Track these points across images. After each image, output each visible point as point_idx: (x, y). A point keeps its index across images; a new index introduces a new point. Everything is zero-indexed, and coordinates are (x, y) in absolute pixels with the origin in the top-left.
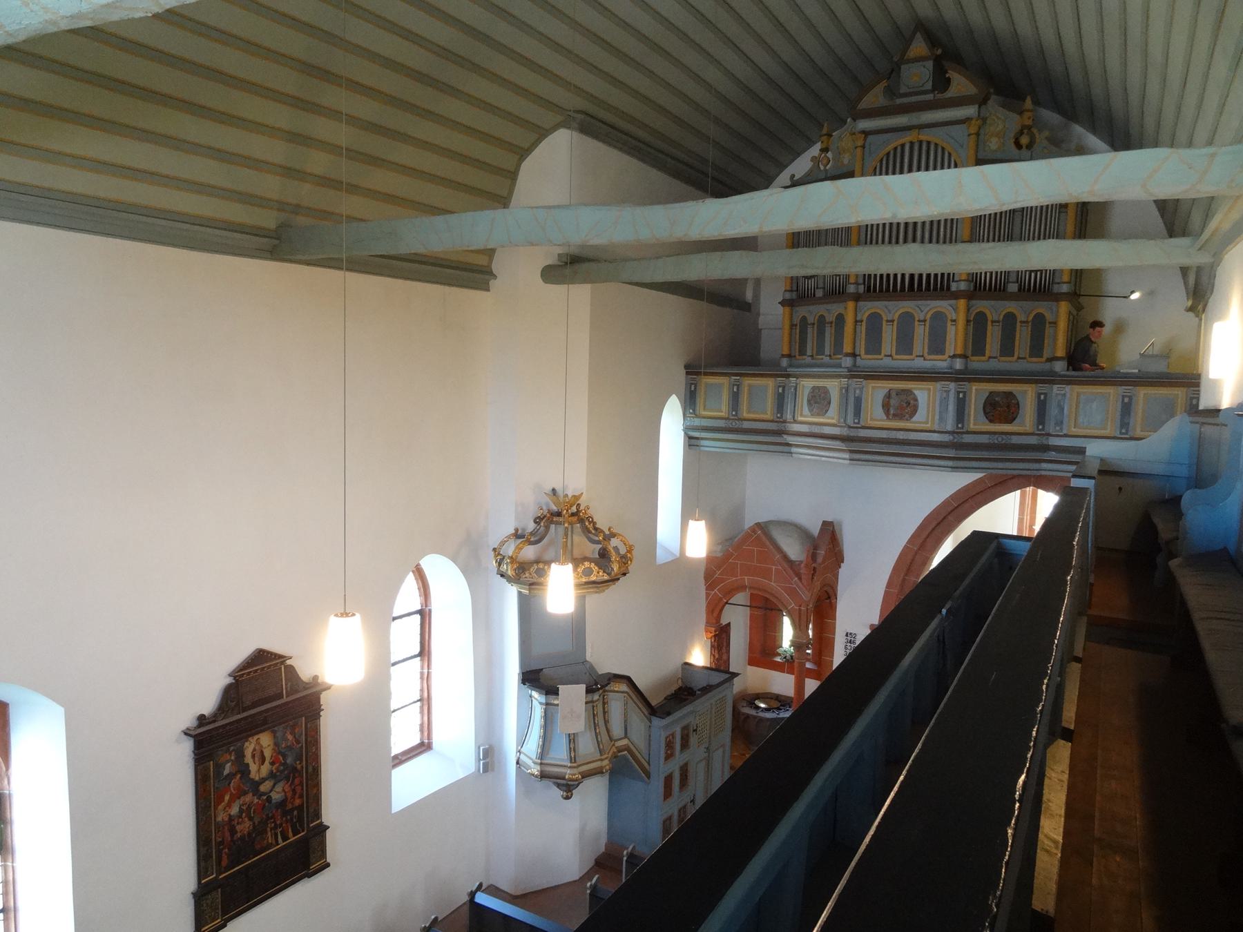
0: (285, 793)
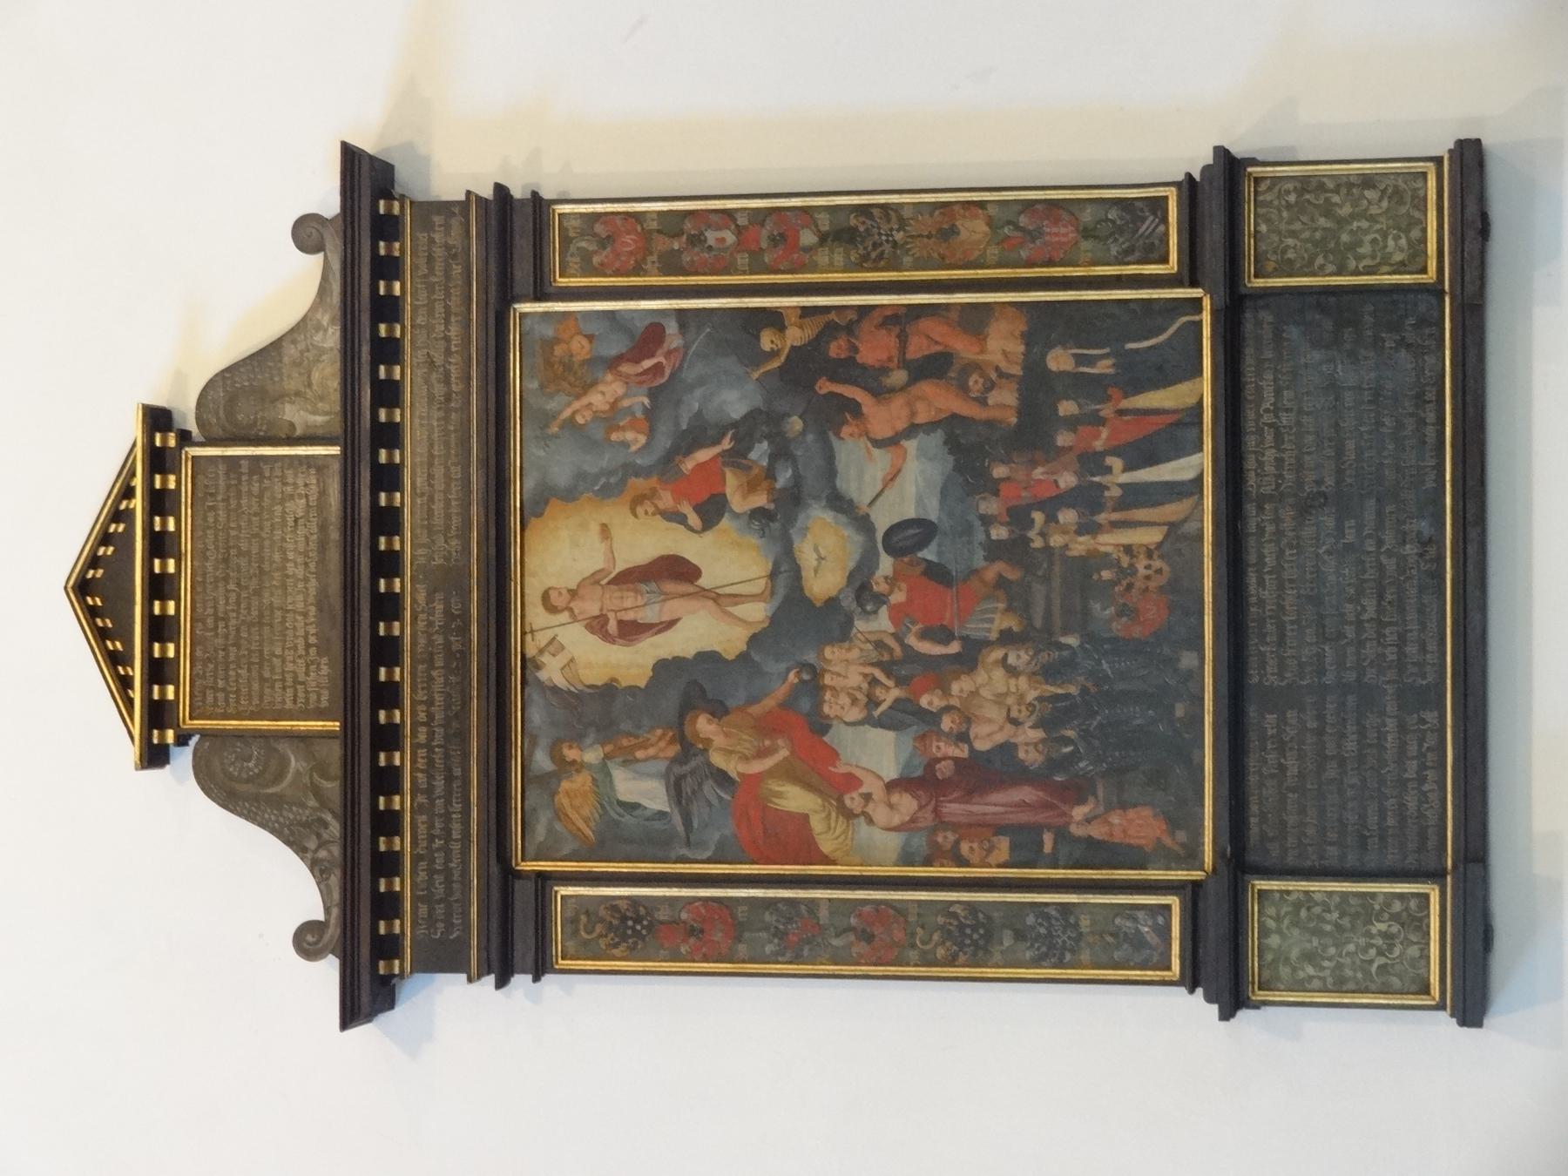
0: (912, 430)
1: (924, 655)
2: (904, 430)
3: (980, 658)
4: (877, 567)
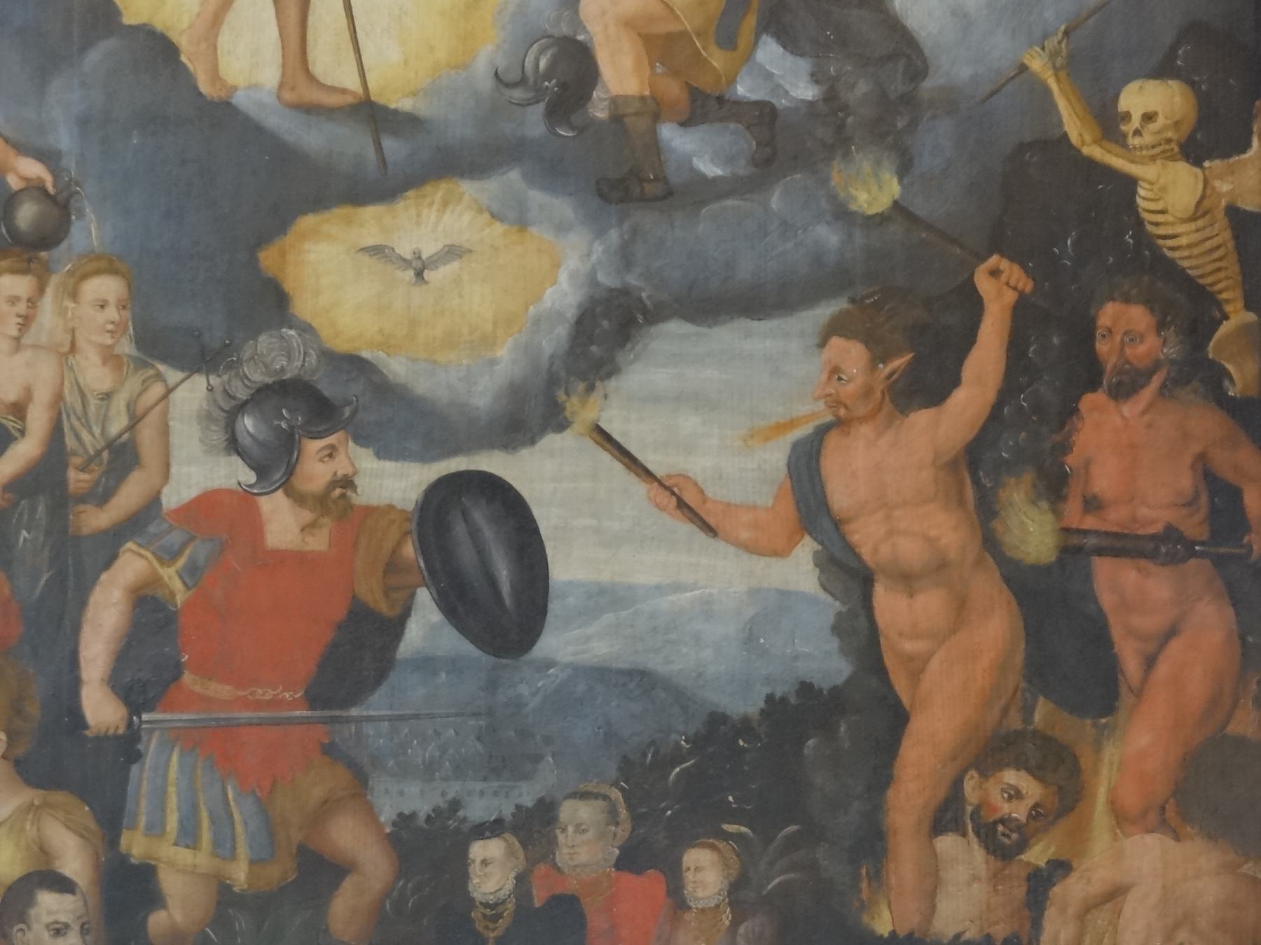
1: (83, 603)
2: (850, 549)
3: (59, 797)
4: (382, 454)
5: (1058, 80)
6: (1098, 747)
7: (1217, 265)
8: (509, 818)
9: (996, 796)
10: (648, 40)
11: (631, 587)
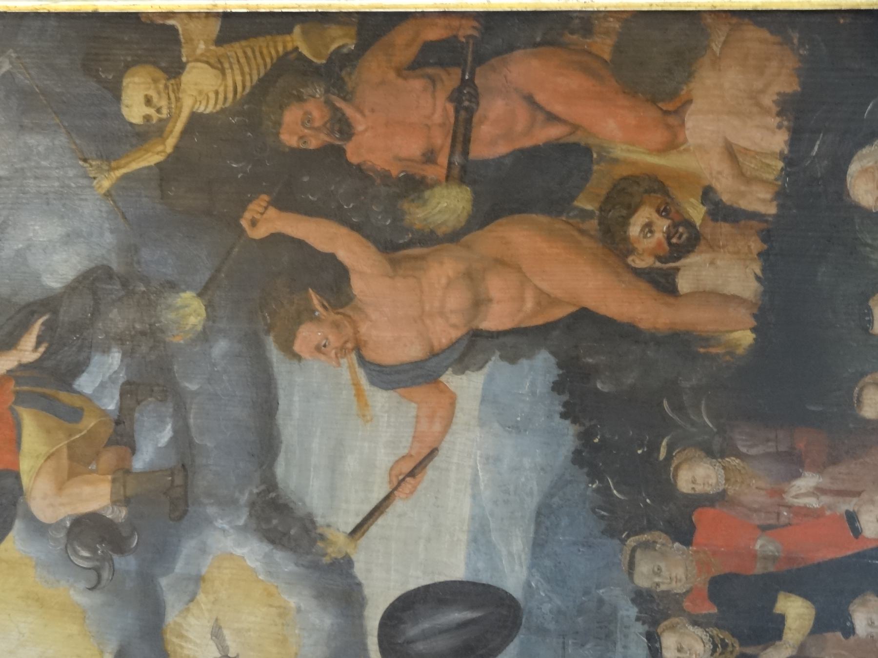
2: (452, 346)
5: (118, 168)
6: (615, 161)
7: (258, 54)
8: (646, 628)
9: (650, 243)
10: (72, 474)
11: (473, 518)
